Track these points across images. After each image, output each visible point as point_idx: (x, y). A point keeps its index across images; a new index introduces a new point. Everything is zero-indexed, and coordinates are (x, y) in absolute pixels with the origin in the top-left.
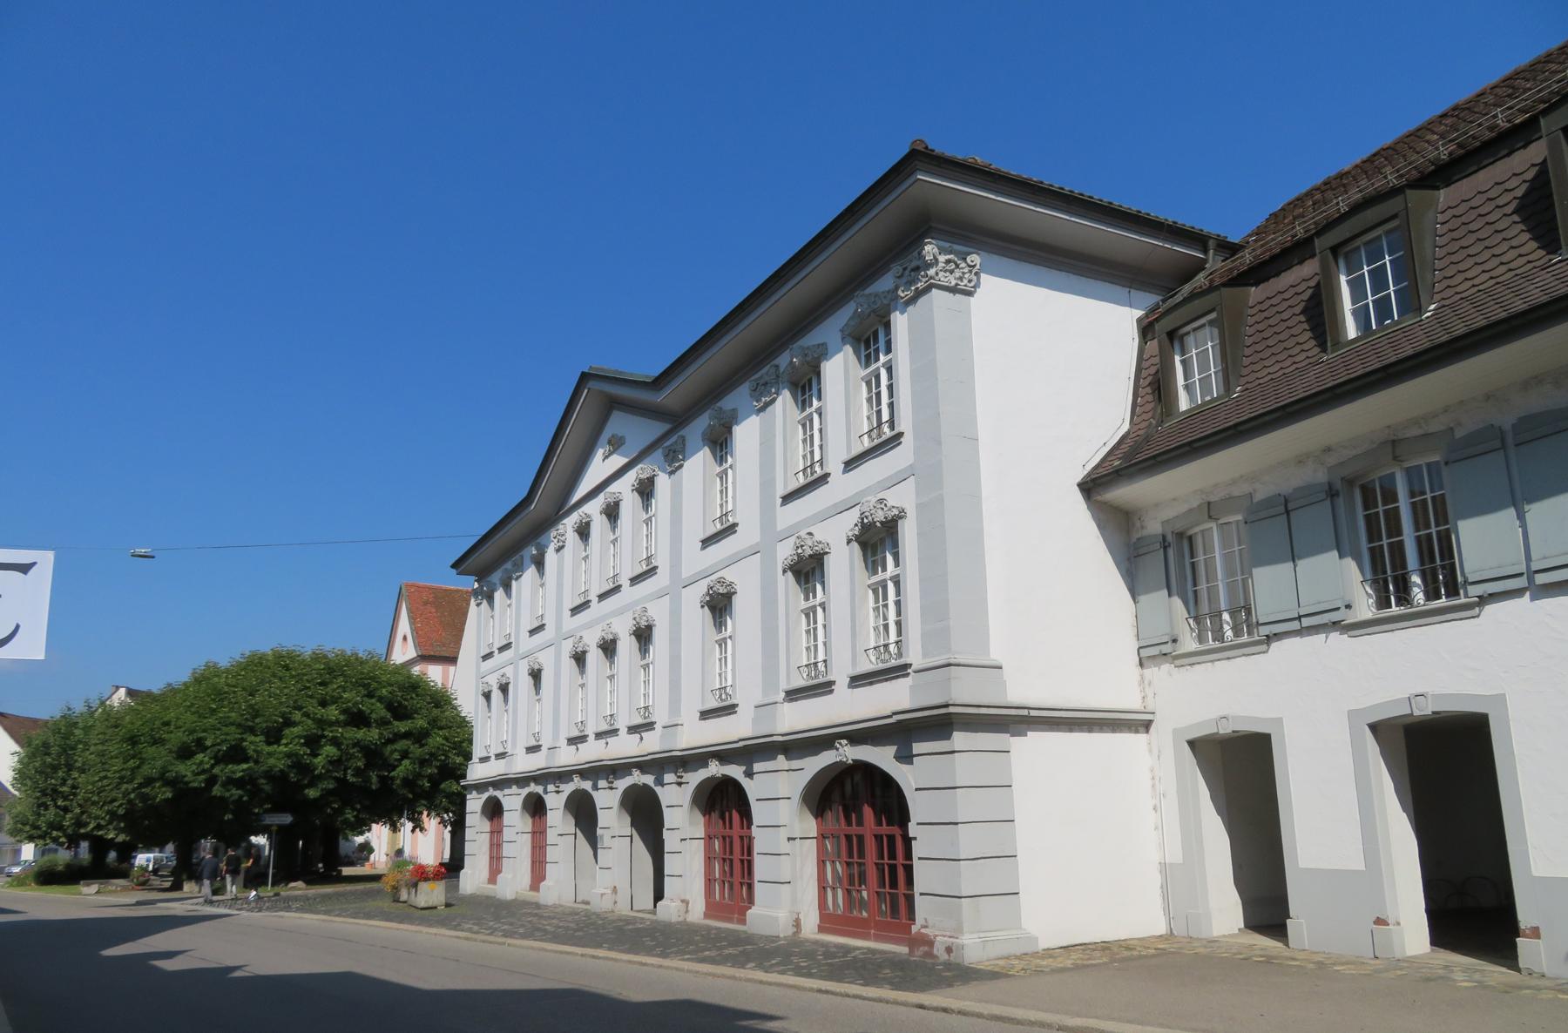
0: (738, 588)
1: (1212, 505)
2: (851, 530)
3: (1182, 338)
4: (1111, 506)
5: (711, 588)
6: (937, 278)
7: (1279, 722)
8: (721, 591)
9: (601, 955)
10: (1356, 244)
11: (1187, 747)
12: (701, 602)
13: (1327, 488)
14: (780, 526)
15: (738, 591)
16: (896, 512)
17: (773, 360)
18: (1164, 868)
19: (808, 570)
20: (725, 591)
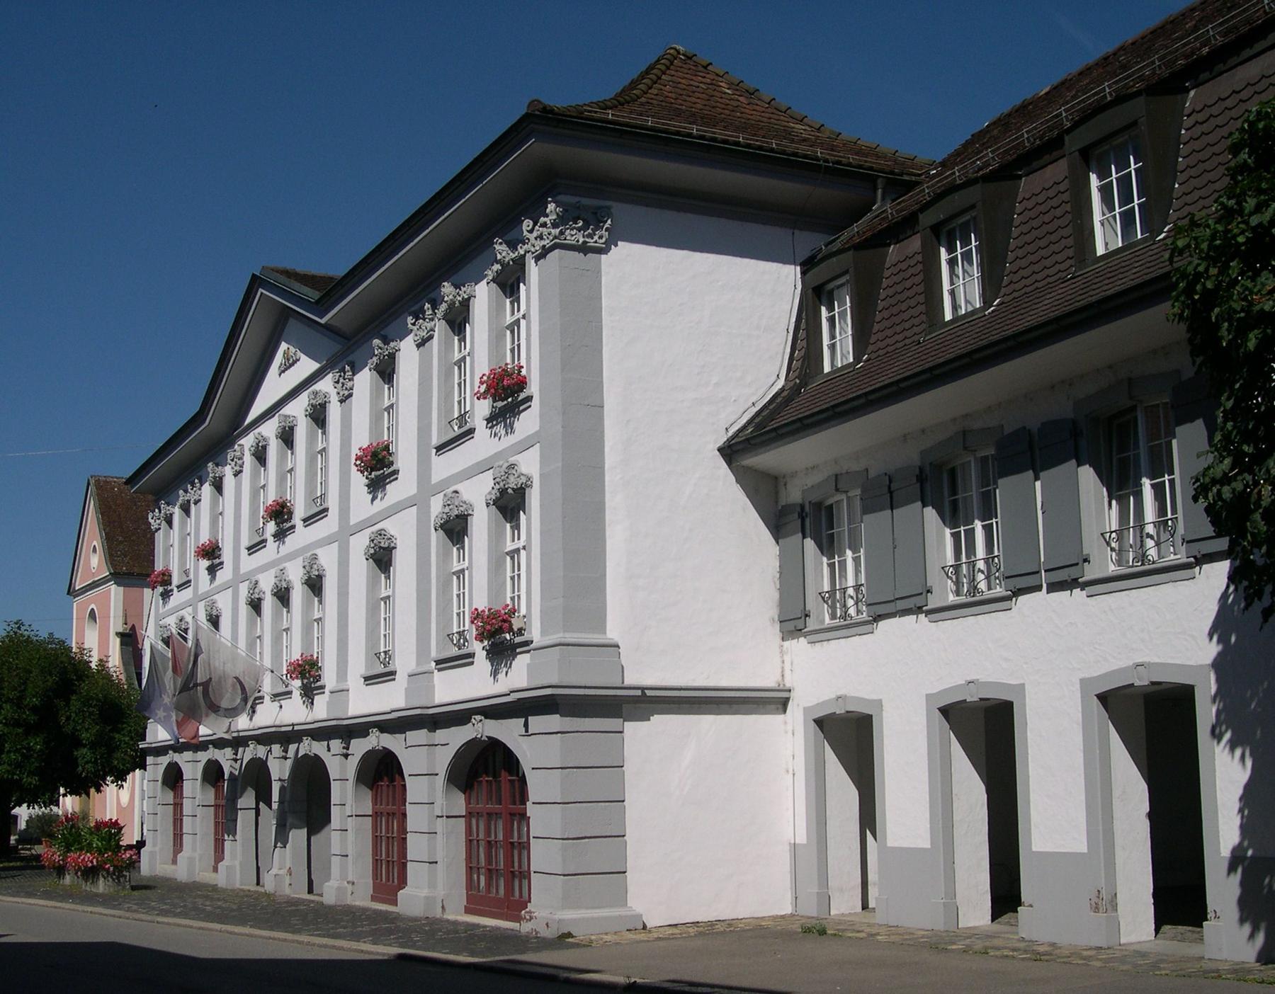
0: (399, 543)
1: (839, 477)
2: (490, 493)
3: (831, 293)
4: (756, 470)
5: (373, 541)
6: (562, 237)
7: (879, 703)
8: (382, 545)
9: (144, 918)
10: (951, 226)
11: (938, 714)
12: (365, 554)
13: (917, 471)
14: (435, 478)
15: (398, 547)
16: (523, 479)
17: (430, 293)
18: (794, 847)
19: (455, 528)
20: (386, 545)
